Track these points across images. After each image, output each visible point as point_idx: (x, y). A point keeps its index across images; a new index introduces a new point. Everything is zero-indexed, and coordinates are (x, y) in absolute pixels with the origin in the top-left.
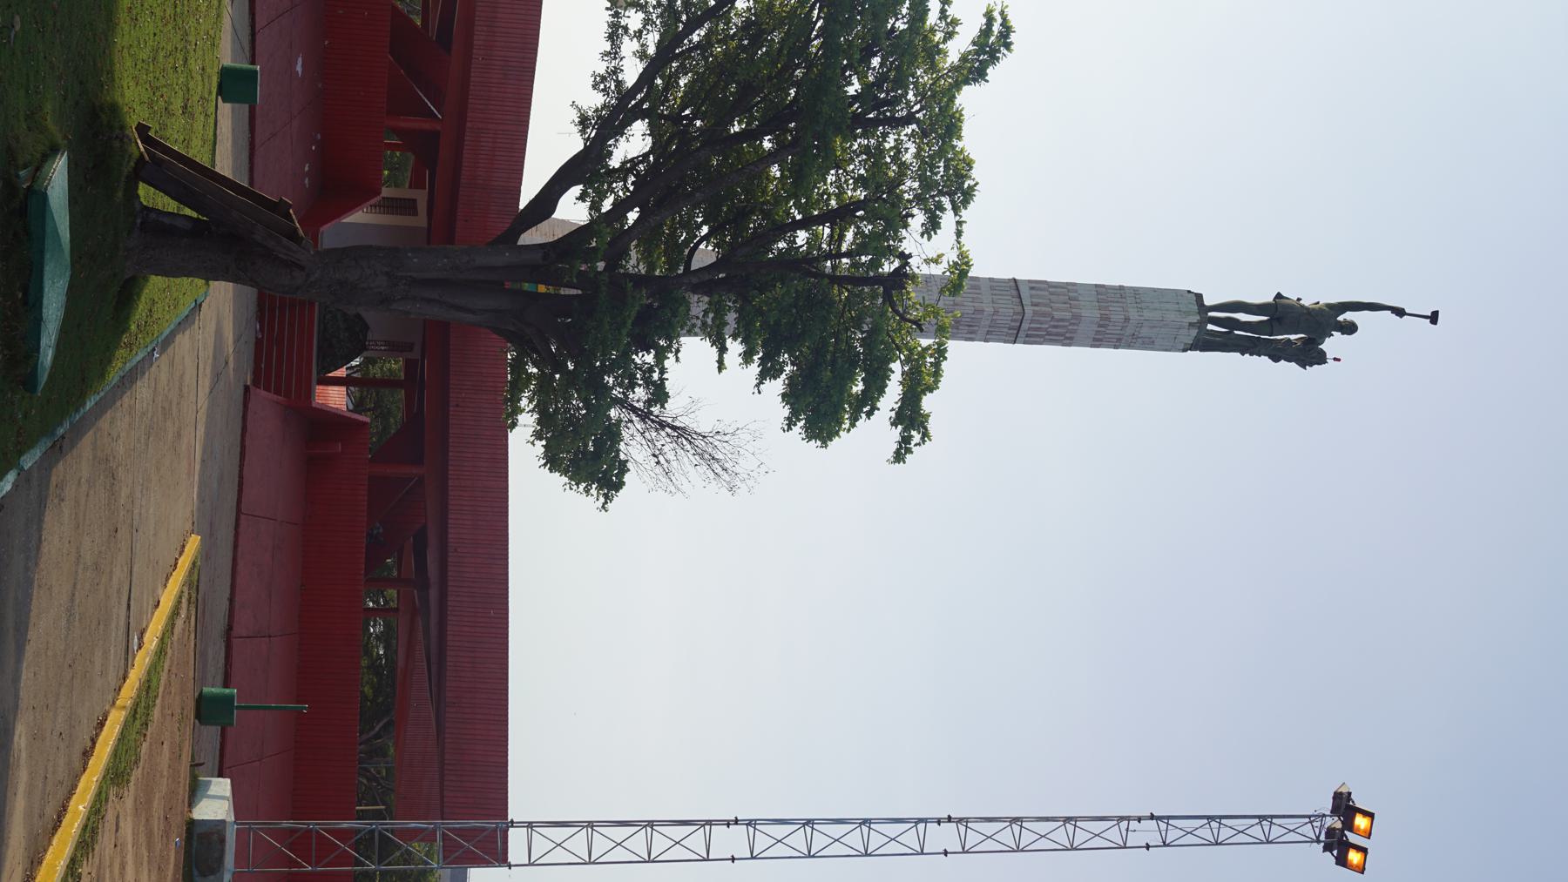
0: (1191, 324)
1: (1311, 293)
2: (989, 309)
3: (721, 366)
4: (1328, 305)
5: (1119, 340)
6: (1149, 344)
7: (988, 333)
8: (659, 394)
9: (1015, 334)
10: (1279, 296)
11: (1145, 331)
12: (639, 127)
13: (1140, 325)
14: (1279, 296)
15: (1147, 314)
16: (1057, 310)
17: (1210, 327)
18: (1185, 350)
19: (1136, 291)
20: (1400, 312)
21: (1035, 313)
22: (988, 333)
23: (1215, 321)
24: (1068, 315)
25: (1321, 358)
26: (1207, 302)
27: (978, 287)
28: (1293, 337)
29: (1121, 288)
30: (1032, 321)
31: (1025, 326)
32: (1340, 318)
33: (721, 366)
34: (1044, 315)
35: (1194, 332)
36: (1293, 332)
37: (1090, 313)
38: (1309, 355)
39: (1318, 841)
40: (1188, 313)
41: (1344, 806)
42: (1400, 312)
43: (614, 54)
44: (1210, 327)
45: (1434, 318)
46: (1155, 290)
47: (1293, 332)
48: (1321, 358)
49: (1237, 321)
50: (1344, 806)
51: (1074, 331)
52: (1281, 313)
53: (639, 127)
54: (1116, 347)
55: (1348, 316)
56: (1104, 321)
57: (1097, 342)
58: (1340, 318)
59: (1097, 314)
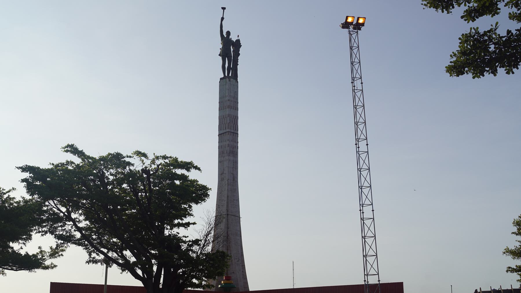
0: (229, 81)
2: (228, 142)
3: (194, 224)
4: (222, 40)
6: (236, 93)
8: (196, 242)
10: (220, 55)
12: (124, 252)
14: (220, 55)
15: (227, 94)
17: (230, 75)
18: (238, 82)
19: (220, 98)
20: (222, 19)
21: (228, 128)
23: (228, 74)
25: (238, 41)
28: (232, 50)
29: (219, 103)
30: (231, 129)
31: (232, 131)
32: (225, 36)
33: (194, 224)
35: (232, 80)
36: (230, 50)
37: (227, 112)
38: (237, 45)
39: (357, 32)
40: (226, 82)
41: (346, 25)
42: (222, 19)
43: (99, 261)
44: (230, 75)
47: (230, 50)
48: (238, 41)
50: (346, 25)
52: (225, 54)
53: (124, 252)
55: (225, 34)
56: (230, 107)
57: (237, 109)
58: (225, 36)
59: (227, 109)
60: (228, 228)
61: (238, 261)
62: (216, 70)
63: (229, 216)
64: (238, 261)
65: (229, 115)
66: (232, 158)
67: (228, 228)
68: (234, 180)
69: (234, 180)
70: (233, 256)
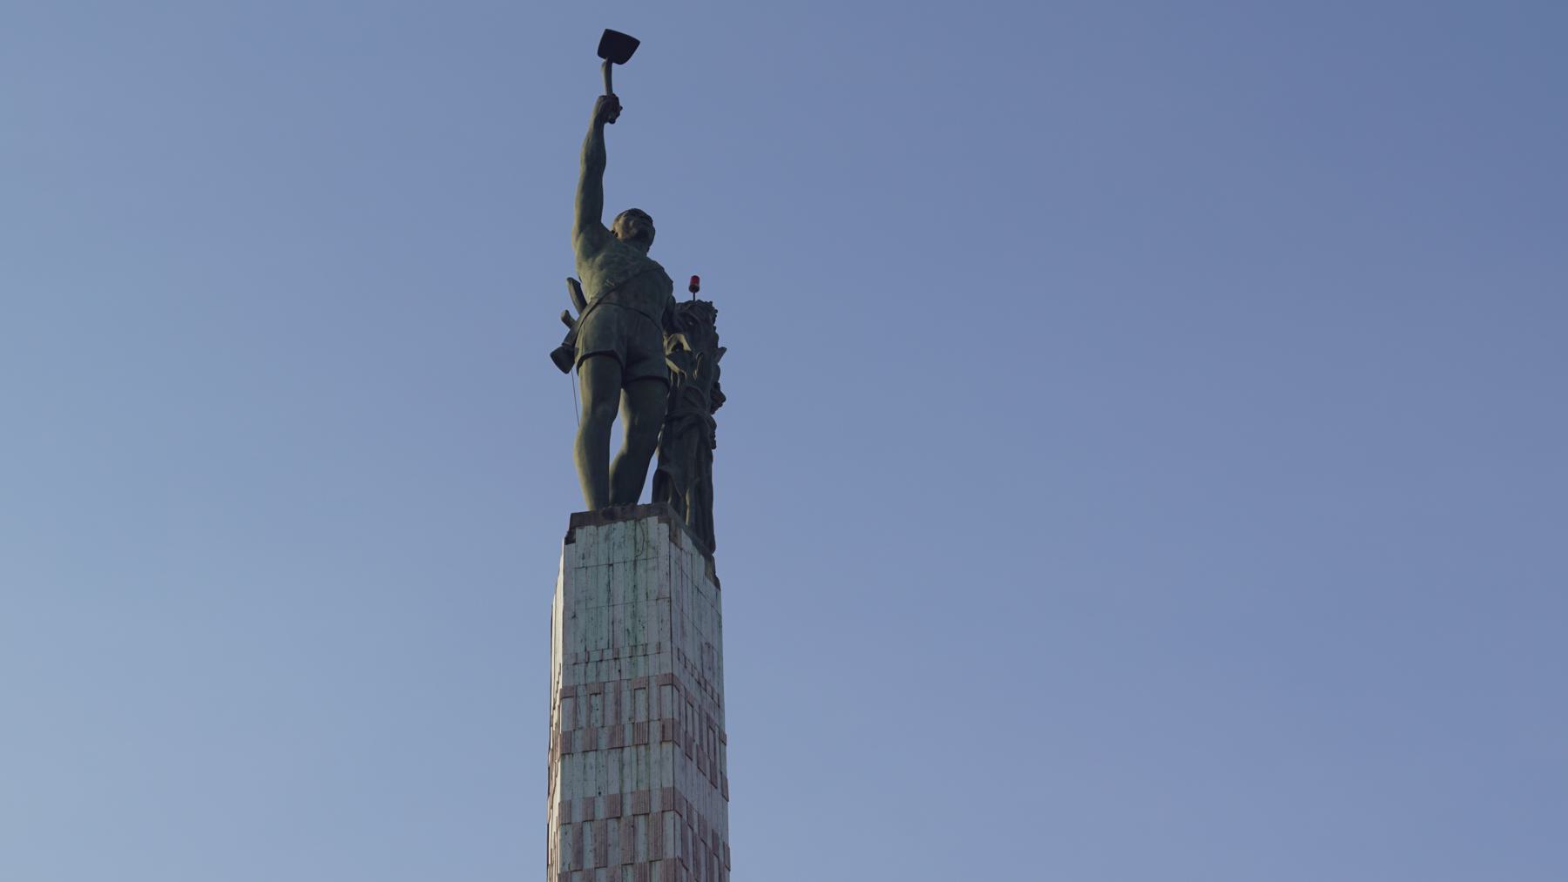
0: (673, 538)
10: (564, 358)
13: (680, 655)
14: (564, 358)
16: (657, 844)
18: (717, 583)
20: (609, 109)
26: (584, 505)
37: (663, 768)
40: (642, 547)
42: (609, 109)
45: (617, 47)
49: (623, 460)
55: (610, 219)
62: (550, 420)
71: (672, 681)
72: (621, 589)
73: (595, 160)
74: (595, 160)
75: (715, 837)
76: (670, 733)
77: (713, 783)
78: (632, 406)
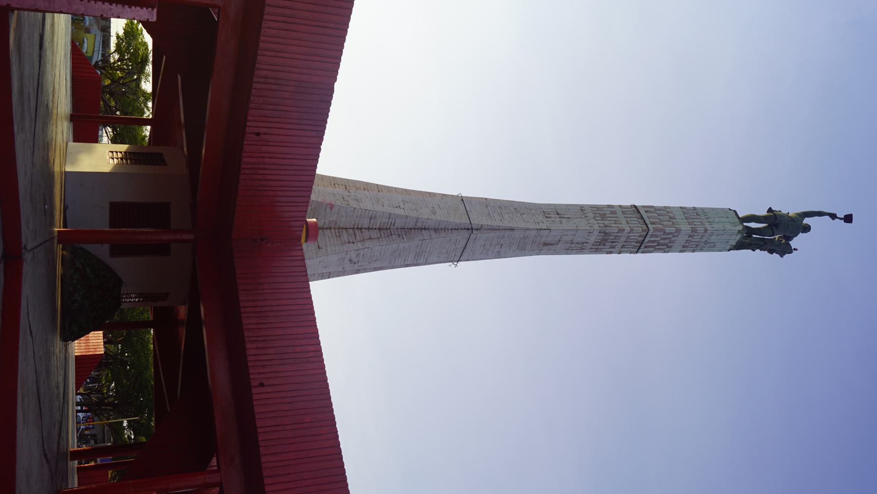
0: (739, 231)
1: (789, 208)
2: (628, 229)
4: (798, 214)
5: (697, 246)
7: (623, 247)
9: (641, 246)
10: (770, 210)
11: (713, 239)
14: (770, 210)
15: (716, 226)
16: (667, 226)
19: (703, 209)
20: (833, 216)
21: (655, 230)
22: (623, 247)
24: (672, 230)
27: (613, 213)
29: (695, 209)
30: (652, 236)
31: (647, 239)
34: (660, 230)
36: (773, 233)
38: (784, 249)
42: (833, 216)
45: (848, 219)
46: (713, 209)
51: (673, 242)
54: (693, 251)
55: (807, 221)
57: (684, 249)
59: (689, 227)
60: (436, 230)
61: (350, 261)
63: (466, 234)
64: (350, 261)
65: (678, 231)
66: (593, 239)
67: (436, 230)
68: (545, 244)
69: (545, 244)
70: (368, 244)
71: (706, 230)
72: (723, 219)
73: (820, 214)
74: (820, 214)
75: (670, 247)
76: (694, 230)
77: (684, 247)
78: (764, 228)
